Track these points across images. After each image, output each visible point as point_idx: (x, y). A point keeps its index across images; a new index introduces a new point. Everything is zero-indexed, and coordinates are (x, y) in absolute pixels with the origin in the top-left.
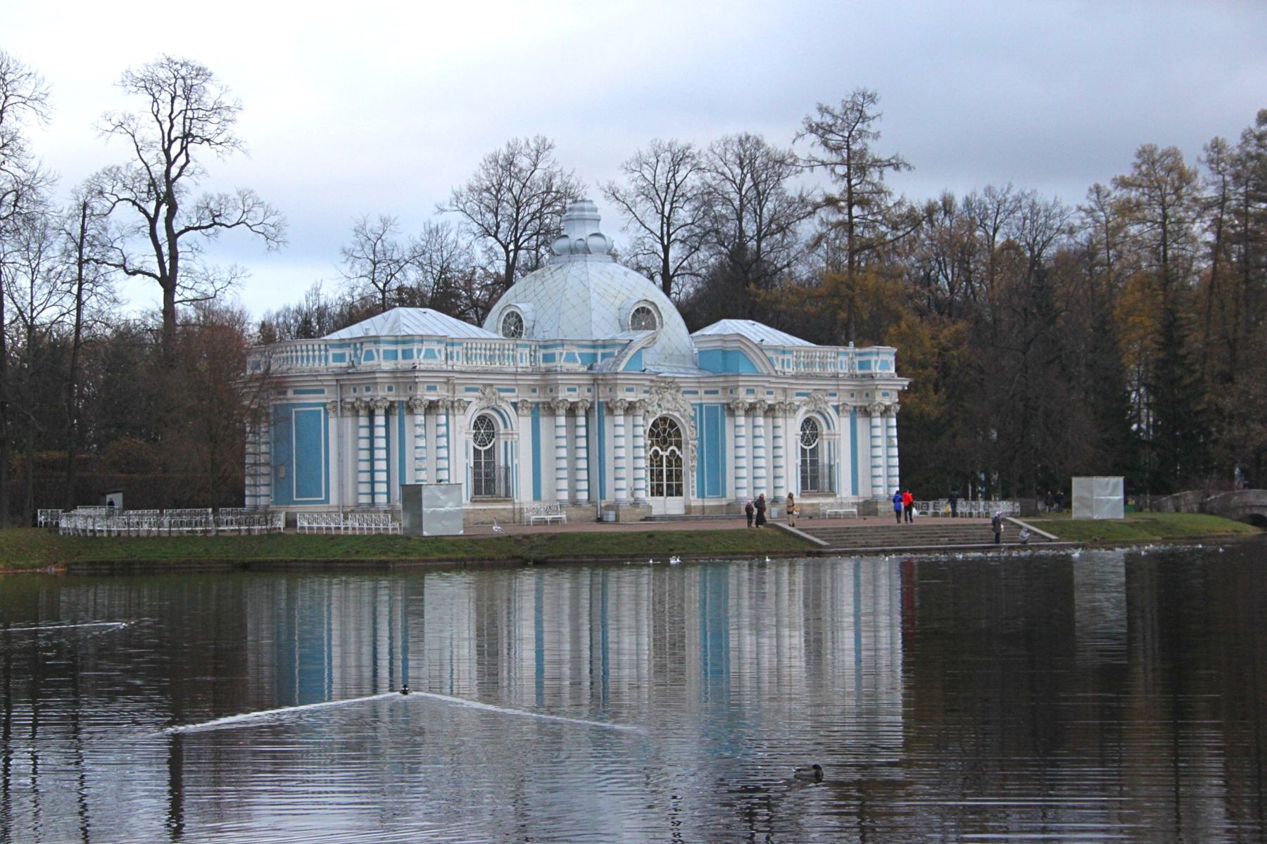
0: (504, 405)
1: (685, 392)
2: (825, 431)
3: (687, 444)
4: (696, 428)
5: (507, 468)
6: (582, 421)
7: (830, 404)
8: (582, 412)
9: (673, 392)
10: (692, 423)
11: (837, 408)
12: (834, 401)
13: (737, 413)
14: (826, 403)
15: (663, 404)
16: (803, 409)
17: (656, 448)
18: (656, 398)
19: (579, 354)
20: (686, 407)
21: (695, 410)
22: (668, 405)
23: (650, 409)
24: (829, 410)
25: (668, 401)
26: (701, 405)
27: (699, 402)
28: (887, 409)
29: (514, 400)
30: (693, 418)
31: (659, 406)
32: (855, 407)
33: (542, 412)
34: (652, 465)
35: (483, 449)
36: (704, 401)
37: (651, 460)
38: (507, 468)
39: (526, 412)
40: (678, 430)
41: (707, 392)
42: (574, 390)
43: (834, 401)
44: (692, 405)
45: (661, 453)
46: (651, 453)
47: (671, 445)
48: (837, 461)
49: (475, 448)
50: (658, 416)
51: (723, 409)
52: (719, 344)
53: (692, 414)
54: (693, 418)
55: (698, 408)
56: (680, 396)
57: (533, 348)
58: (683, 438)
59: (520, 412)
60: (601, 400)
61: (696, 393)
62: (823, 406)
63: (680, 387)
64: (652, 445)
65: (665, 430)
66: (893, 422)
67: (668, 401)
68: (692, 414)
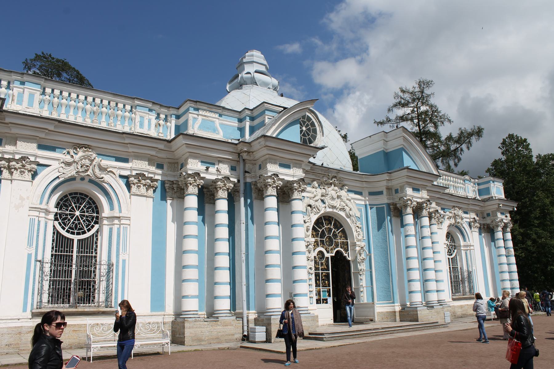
0: (107, 178)
2: (462, 243)
3: (354, 245)
5: (110, 266)
6: (222, 205)
7: (465, 220)
8: (223, 194)
14: (462, 219)
15: (327, 200)
17: (320, 249)
18: (320, 191)
19: (221, 125)
21: (360, 210)
23: (312, 202)
24: (464, 225)
25: (333, 199)
29: (126, 173)
31: (323, 201)
34: (316, 269)
35: (76, 238)
38: (110, 266)
39: (143, 190)
40: (343, 232)
45: (327, 255)
47: (337, 246)
48: (474, 268)
49: (56, 233)
51: (389, 209)
53: (358, 215)
59: (134, 189)
60: (249, 180)
65: (330, 230)
66: (509, 236)
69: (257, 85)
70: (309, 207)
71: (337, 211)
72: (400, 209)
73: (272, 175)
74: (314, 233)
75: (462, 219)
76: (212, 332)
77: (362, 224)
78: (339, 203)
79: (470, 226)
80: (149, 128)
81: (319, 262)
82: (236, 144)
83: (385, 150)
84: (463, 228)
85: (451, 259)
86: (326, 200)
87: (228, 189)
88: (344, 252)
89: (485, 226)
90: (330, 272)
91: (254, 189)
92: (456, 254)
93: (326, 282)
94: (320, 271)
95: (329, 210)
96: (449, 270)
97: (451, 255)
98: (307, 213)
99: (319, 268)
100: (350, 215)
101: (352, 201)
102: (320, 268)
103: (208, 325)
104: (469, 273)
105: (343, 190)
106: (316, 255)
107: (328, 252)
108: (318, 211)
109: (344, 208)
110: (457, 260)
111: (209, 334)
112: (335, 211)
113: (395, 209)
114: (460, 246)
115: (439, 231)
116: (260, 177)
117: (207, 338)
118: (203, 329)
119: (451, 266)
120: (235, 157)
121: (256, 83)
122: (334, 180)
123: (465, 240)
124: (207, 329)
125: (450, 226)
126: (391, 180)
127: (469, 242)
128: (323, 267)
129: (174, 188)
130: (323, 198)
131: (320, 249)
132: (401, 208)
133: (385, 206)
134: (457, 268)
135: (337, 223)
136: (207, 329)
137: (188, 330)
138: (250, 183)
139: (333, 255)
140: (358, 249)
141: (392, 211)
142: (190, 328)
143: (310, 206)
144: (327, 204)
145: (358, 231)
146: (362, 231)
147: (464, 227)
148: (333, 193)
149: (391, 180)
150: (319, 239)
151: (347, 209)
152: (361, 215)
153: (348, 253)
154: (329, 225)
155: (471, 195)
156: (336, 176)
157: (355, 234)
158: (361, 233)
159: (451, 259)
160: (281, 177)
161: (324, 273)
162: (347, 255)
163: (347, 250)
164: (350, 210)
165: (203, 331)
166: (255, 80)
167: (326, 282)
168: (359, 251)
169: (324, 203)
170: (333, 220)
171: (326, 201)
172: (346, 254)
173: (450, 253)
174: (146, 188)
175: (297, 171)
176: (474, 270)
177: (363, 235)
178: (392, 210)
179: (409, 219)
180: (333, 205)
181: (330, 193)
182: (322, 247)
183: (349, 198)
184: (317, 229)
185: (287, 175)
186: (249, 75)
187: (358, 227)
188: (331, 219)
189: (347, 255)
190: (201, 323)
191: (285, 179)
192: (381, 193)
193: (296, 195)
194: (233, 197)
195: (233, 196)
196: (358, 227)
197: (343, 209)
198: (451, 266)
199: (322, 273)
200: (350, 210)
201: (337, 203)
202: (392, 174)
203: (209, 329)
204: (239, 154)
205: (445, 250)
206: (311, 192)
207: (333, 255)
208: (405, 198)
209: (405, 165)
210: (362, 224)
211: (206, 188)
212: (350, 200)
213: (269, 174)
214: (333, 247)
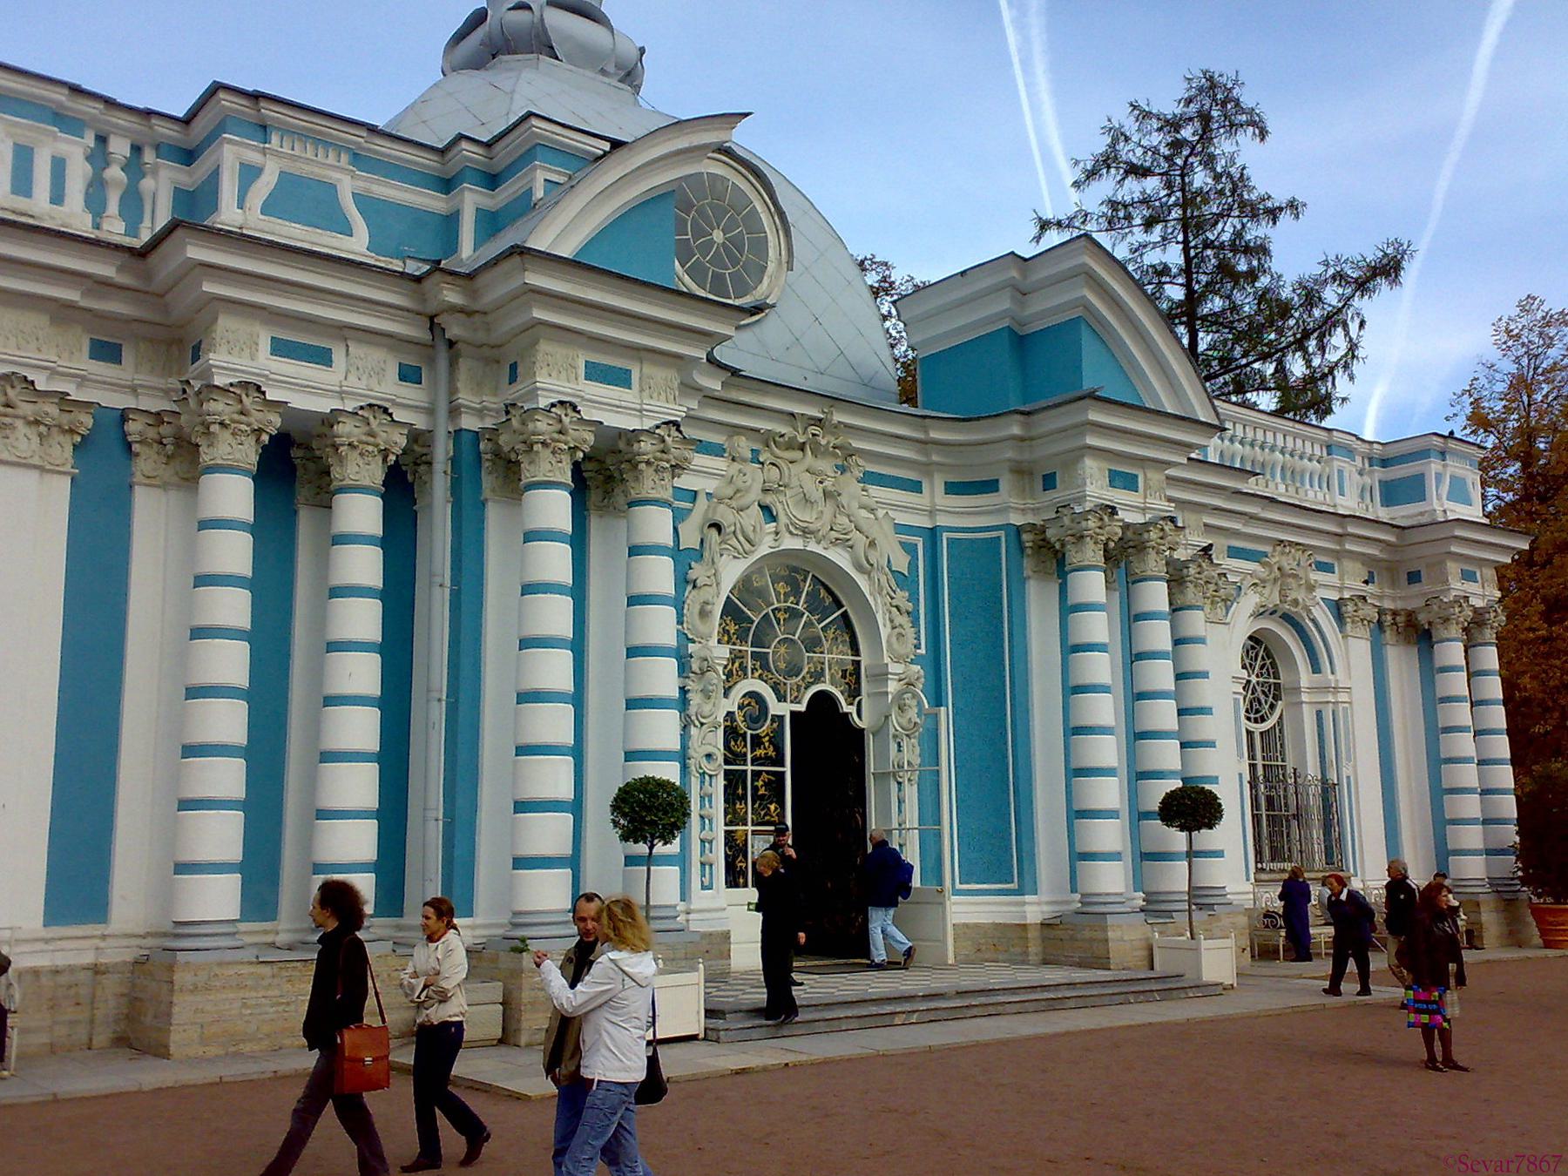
1: (870, 478)
2: (1305, 677)
3: (881, 676)
4: (913, 616)
7: (1320, 593)
9: (826, 465)
10: (901, 597)
11: (1337, 609)
12: (1328, 586)
13: (1073, 557)
14: (1311, 588)
15: (786, 506)
16: (1250, 602)
17: (753, 684)
18: (754, 478)
19: (361, 200)
20: (875, 532)
21: (910, 549)
22: (806, 516)
23: (725, 516)
24: (1316, 612)
25: (807, 501)
26: (933, 534)
27: (926, 523)
28: (1478, 620)
30: (905, 580)
32: (1381, 612)
33: (147, 462)
34: (732, 757)
36: (942, 521)
37: (732, 733)
41: (952, 488)
42: (322, 357)
43: (1328, 586)
44: (900, 528)
45: (776, 708)
46: (732, 703)
48: (1345, 772)
50: (764, 550)
52: (1004, 303)
53: (901, 563)
54: (905, 580)
55: (920, 542)
56: (851, 488)
57: (119, 147)
58: (865, 660)
60: (469, 422)
61: (916, 487)
62: (1300, 595)
63: (850, 453)
64: (732, 677)
66: (1490, 657)
67: (807, 501)
68: (901, 563)
69: (557, 58)
70: (714, 532)
71: (818, 549)
72: (1058, 546)
73: (553, 405)
74: (732, 628)
75: (1311, 588)
76: (288, 1004)
77: (914, 598)
78: (827, 516)
79: (1340, 618)
80: (57, 197)
81: (745, 733)
82: (418, 280)
83: (1016, 328)
84: (1310, 624)
85: (1261, 733)
86: (779, 506)
87: (385, 453)
88: (841, 698)
89: (1398, 619)
90: (788, 769)
91: (489, 456)
92: (1281, 717)
93: (772, 807)
94: (749, 768)
95: (791, 543)
96: (1247, 777)
97: (1263, 720)
98: (706, 554)
99: (745, 754)
100: (872, 565)
101: (881, 513)
102: (749, 757)
103: (273, 976)
104: (1328, 790)
105: (848, 474)
106: (735, 709)
107: (781, 698)
108: (747, 546)
109: (849, 540)
110: (1282, 738)
111: (277, 1012)
112: (813, 547)
113: (1040, 547)
114: (1297, 690)
115: (1214, 634)
116: (507, 413)
117: (266, 1029)
118: (254, 994)
119: (1259, 762)
120: (418, 332)
121: (552, 48)
122: (814, 435)
123: (1316, 668)
124: (270, 993)
125: (1258, 615)
126: (1032, 439)
127: (1331, 677)
128: (758, 752)
129: (165, 441)
130: (769, 499)
131: (753, 684)
132: (1063, 545)
133: (1002, 533)
134: (1284, 767)
135: (823, 592)
136: (270, 993)
137: (190, 998)
138: (477, 436)
139: (802, 708)
140: (893, 687)
141: (1028, 556)
142: (195, 990)
143: (717, 526)
144: (783, 519)
145: (897, 623)
146: (915, 623)
147: (1314, 621)
148: (809, 483)
149: (1032, 439)
150: (750, 649)
151: (859, 540)
152: (913, 565)
153: (860, 702)
154: (792, 598)
155: (1348, 503)
156: (820, 420)
157: (885, 632)
158: (910, 632)
159: (1261, 733)
160: (588, 413)
161: (767, 772)
162: (852, 709)
163: (854, 693)
164: (872, 544)
165: (249, 1002)
166: (549, 39)
167: (772, 807)
168: (900, 695)
169: (774, 518)
170: (805, 581)
171: (778, 509)
172: (851, 704)
173: (1257, 711)
174: (40, 435)
175: (655, 395)
176: (1348, 777)
177: (918, 638)
178: (1029, 551)
179: (1092, 585)
180: (805, 525)
181: (795, 482)
182: (760, 677)
183: (871, 503)
184: (743, 612)
185: (617, 408)
186: (522, 16)
187: (897, 607)
188: (800, 578)
189: (852, 709)
190: (245, 970)
191: (605, 424)
192: (990, 486)
193: (650, 484)
194: (412, 484)
195: (410, 478)
196: (897, 607)
197: (844, 543)
198: (1259, 762)
199: (756, 775)
200: (872, 544)
201: (818, 516)
202: (1035, 418)
203: (277, 992)
204: (432, 318)
205: (1236, 700)
206: (722, 476)
207: (802, 708)
208: (1078, 509)
209: (1087, 385)
210: (914, 598)
211: (299, 446)
212: (872, 511)
213: (543, 403)
214: (804, 678)
